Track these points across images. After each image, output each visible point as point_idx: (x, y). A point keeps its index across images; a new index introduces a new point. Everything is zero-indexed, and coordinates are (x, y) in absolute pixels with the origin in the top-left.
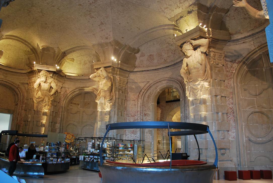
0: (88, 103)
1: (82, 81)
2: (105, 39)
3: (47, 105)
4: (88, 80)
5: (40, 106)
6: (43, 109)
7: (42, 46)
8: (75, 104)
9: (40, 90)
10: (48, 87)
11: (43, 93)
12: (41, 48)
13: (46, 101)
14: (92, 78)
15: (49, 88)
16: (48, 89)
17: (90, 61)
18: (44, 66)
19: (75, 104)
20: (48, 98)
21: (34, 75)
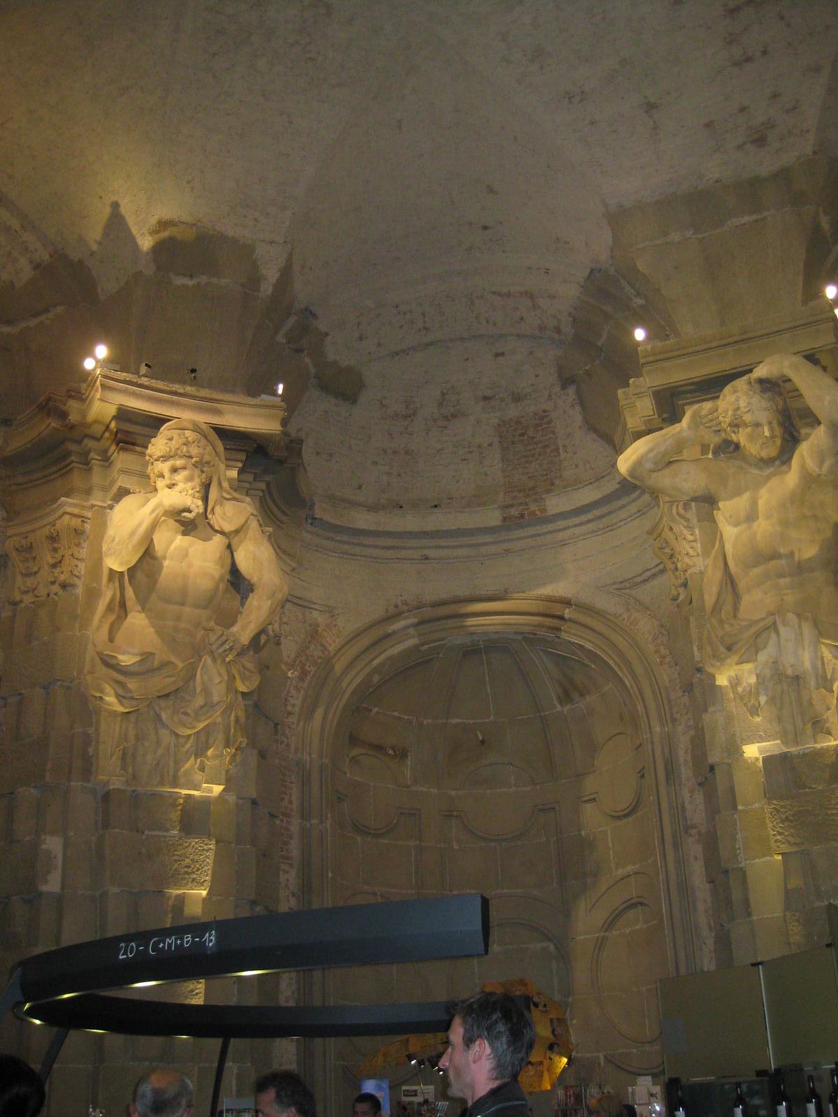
0: (483, 742)
1: (432, 553)
2: (740, 147)
3: (221, 736)
4: (488, 538)
5: (158, 743)
6: (187, 773)
7: (163, 225)
8: (379, 748)
9: (143, 602)
10: (217, 575)
12: (146, 243)
13: (206, 691)
14: (649, 466)
15: (221, 578)
17: (489, 393)
18: (176, 387)
19: (379, 748)
20: (223, 671)
21: (76, 479)
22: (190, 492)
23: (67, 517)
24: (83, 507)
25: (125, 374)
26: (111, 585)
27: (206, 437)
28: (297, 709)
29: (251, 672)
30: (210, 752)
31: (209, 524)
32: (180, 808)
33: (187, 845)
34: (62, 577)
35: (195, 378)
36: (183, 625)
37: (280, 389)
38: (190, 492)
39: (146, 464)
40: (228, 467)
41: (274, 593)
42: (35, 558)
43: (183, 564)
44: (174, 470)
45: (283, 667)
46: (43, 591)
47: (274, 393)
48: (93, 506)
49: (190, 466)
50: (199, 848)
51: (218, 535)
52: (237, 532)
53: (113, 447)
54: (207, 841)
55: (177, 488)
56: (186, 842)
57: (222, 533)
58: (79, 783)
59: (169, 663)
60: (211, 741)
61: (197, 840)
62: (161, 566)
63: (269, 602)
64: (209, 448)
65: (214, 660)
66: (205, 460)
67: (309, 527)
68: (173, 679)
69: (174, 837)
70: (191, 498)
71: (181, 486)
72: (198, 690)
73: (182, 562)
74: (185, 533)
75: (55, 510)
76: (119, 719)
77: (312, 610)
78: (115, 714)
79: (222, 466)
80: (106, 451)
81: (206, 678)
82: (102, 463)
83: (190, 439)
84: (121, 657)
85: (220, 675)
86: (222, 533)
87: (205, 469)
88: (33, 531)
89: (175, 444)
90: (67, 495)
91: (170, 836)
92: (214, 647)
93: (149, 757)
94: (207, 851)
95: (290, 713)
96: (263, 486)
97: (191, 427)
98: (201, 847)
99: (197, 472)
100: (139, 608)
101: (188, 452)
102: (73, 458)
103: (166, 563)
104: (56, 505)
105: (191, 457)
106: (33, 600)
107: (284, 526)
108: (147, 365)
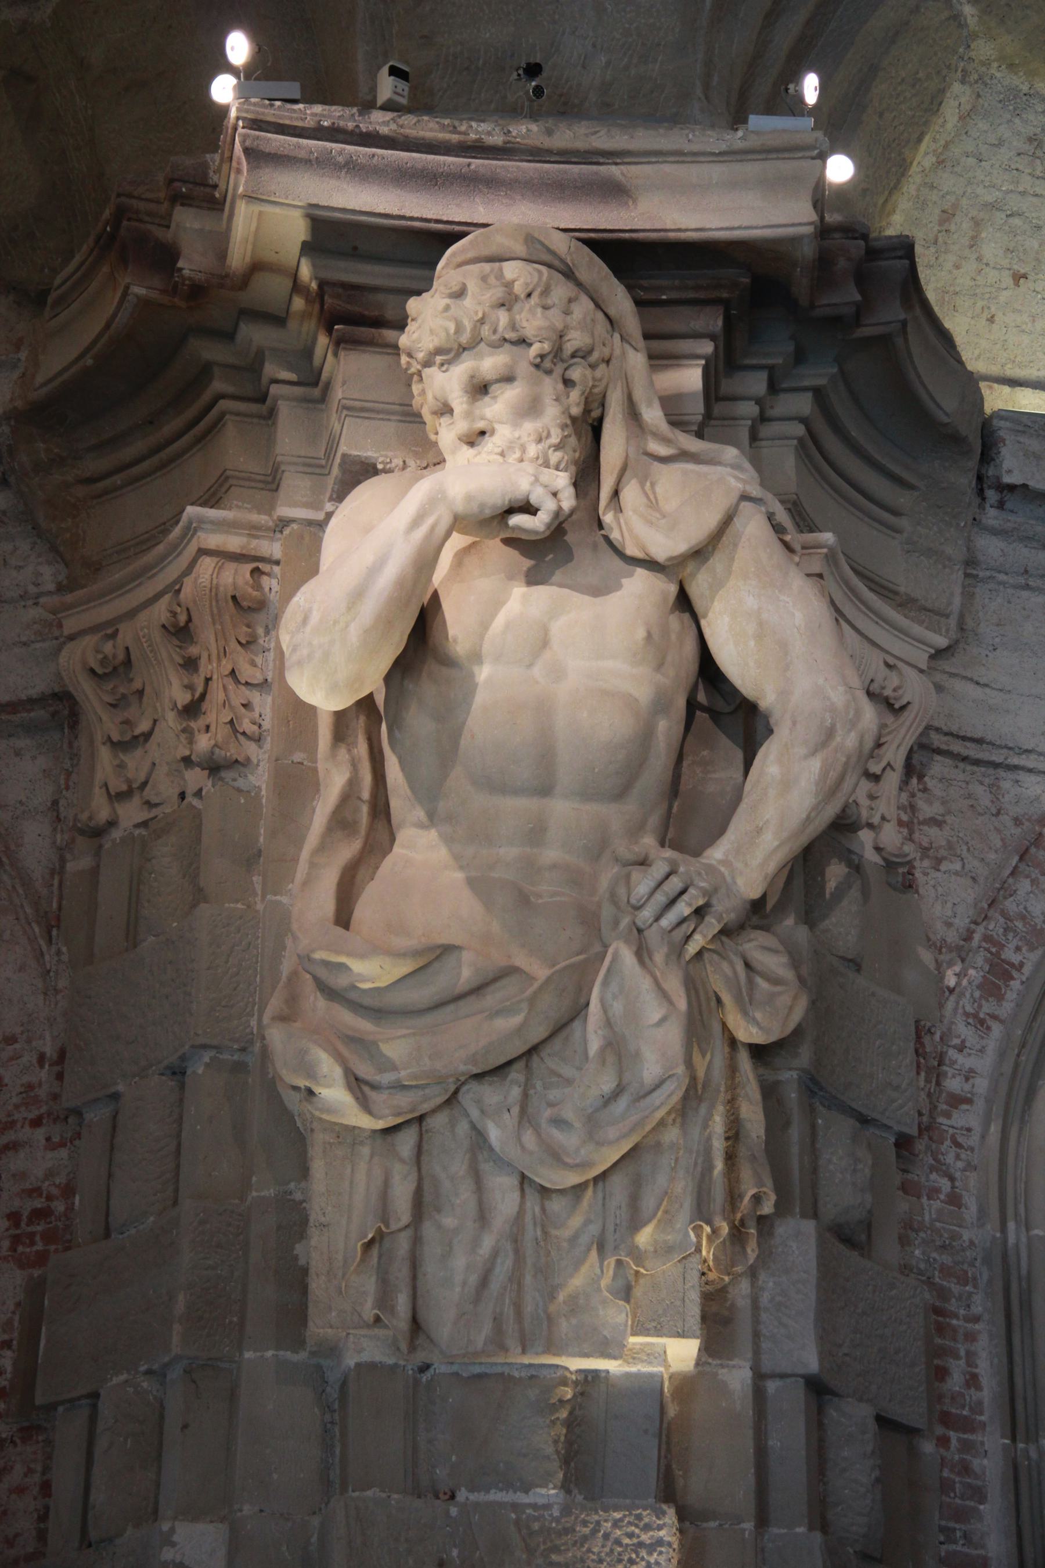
3: (683, 1187)
5: (483, 1217)
6: (574, 1306)
10: (643, 693)
11: (510, 852)
15: (660, 705)
16: (645, 737)
20: (675, 985)
22: (533, 450)
23: (207, 563)
24: (254, 530)
25: (318, 109)
26: (343, 753)
27: (569, 274)
28: (981, 1085)
29: (776, 981)
30: (644, 1237)
31: (607, 538)
32: (563, 1414)
33: (586, 1531)
34: (203, 743)
35: (538, 91)
36: (551, 854)
37: (810, 87)
38: (533, 450)
39: (408, 380)
40: (659, 360)
41: (830, 733)
42: (140, 693)
43: (537, 671)
44: (480, 389)
45: (927, 957)
46: (165, 788)
47: (796, 106)
48: (284, 523)
49: (524, 368)
50: (626, 1541)
51: (640, 572)
52: (700, 554)
53: (323, 340)
54: (648, 1517)
55: (490, 444)
56: (585, 1523)
57: (651, 564)
58: (269, 1354)
59: (509, 971)
60: (648, 1202)
61: (617, 1515)
62: (470, 687)
63: (815, 765)
64: (583, 307)
65: (642, 953)
66: (569, 348)
67: (992, 516)
68: (517, 1020)
69: (547, 1507)
70: (529, 468)
71: (503, 434)
72: (594, 1045)
73: (530, 666)
74: (533, 579)
75: (175, 549)
76: (366, 1151)
77: (1022, 776)
78: (348, 1135)
79: (636, 360)
80: (308, 353)
81: (617, 1008)
82: (298, 391)
83: (518, 288)
84: (358, 966)
85: (664, 995)
86: (651, 564)
87: (575, 374)
88: (132, 614)
89: (471, 306)
90: (212, 500)
91: (535, 1506)
92: (647, 914)
93: (460, 1262)
94: (651, 1548)
95: (957, 1101)
96: (803, 404)
97: (520, 249)
98: (631, 1535)
99: (550, 386)
100: (420, 814)
101: (513, 326)
102: (218, 385)
103: (484, 673)
104: (177, 531)
105: (523, 342)
106: (144, 815)
107: (904, 523)
108: (394, 71)
